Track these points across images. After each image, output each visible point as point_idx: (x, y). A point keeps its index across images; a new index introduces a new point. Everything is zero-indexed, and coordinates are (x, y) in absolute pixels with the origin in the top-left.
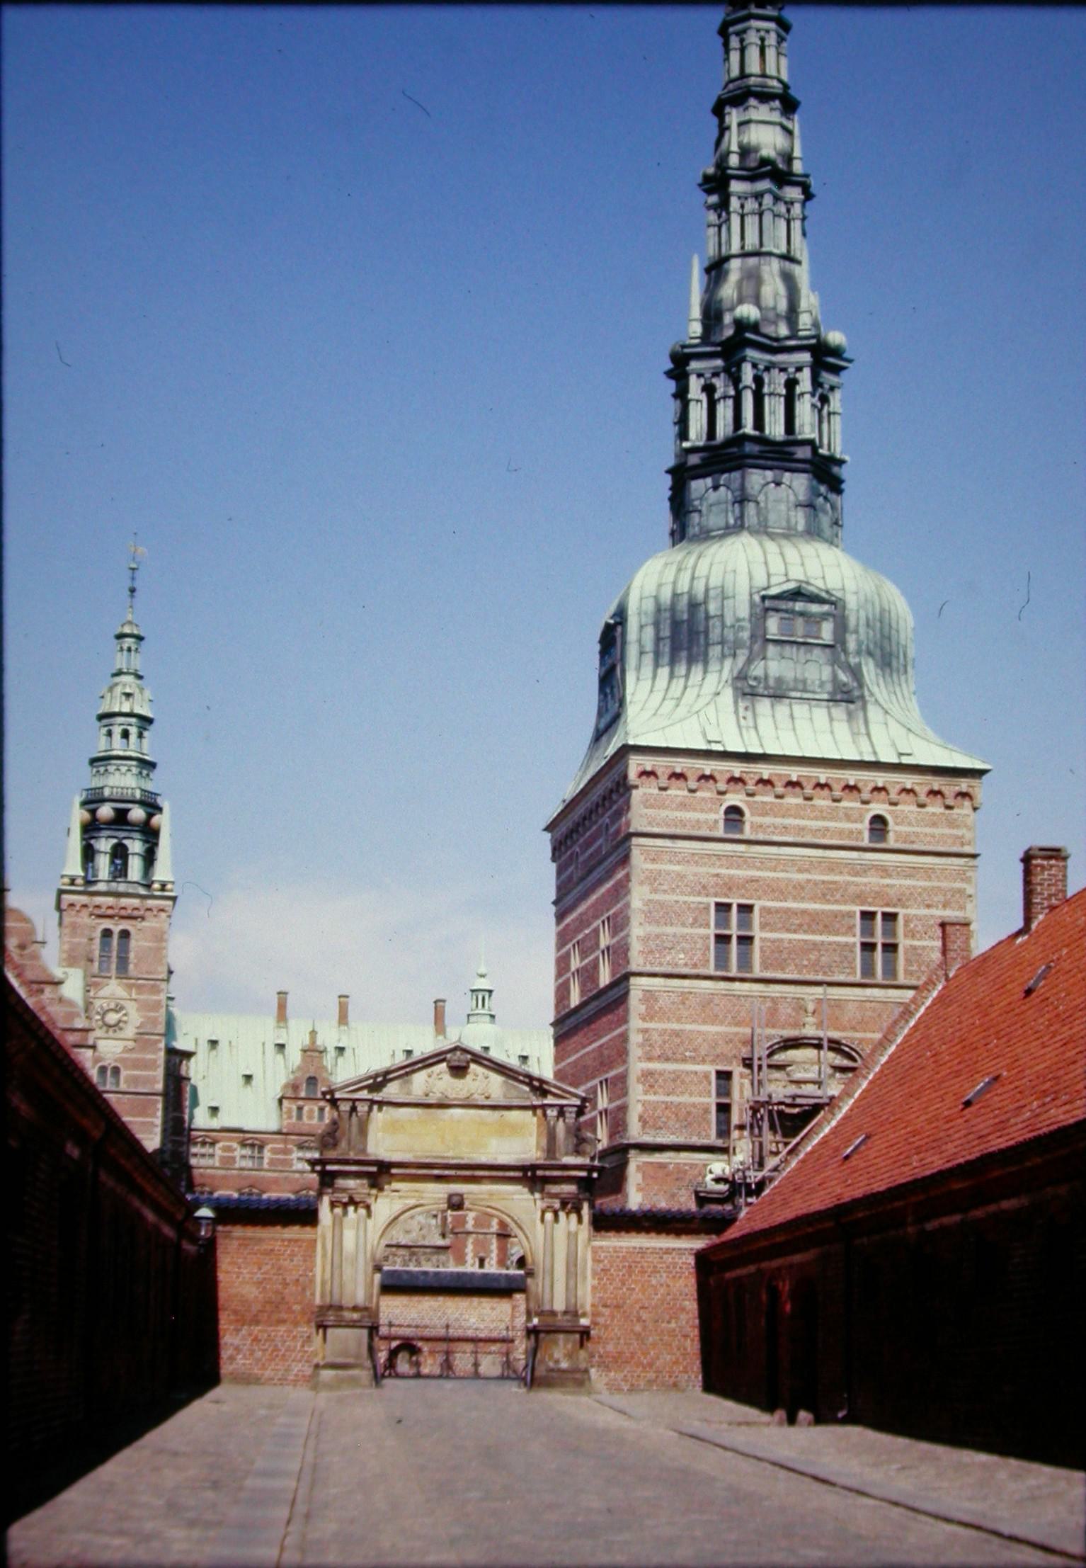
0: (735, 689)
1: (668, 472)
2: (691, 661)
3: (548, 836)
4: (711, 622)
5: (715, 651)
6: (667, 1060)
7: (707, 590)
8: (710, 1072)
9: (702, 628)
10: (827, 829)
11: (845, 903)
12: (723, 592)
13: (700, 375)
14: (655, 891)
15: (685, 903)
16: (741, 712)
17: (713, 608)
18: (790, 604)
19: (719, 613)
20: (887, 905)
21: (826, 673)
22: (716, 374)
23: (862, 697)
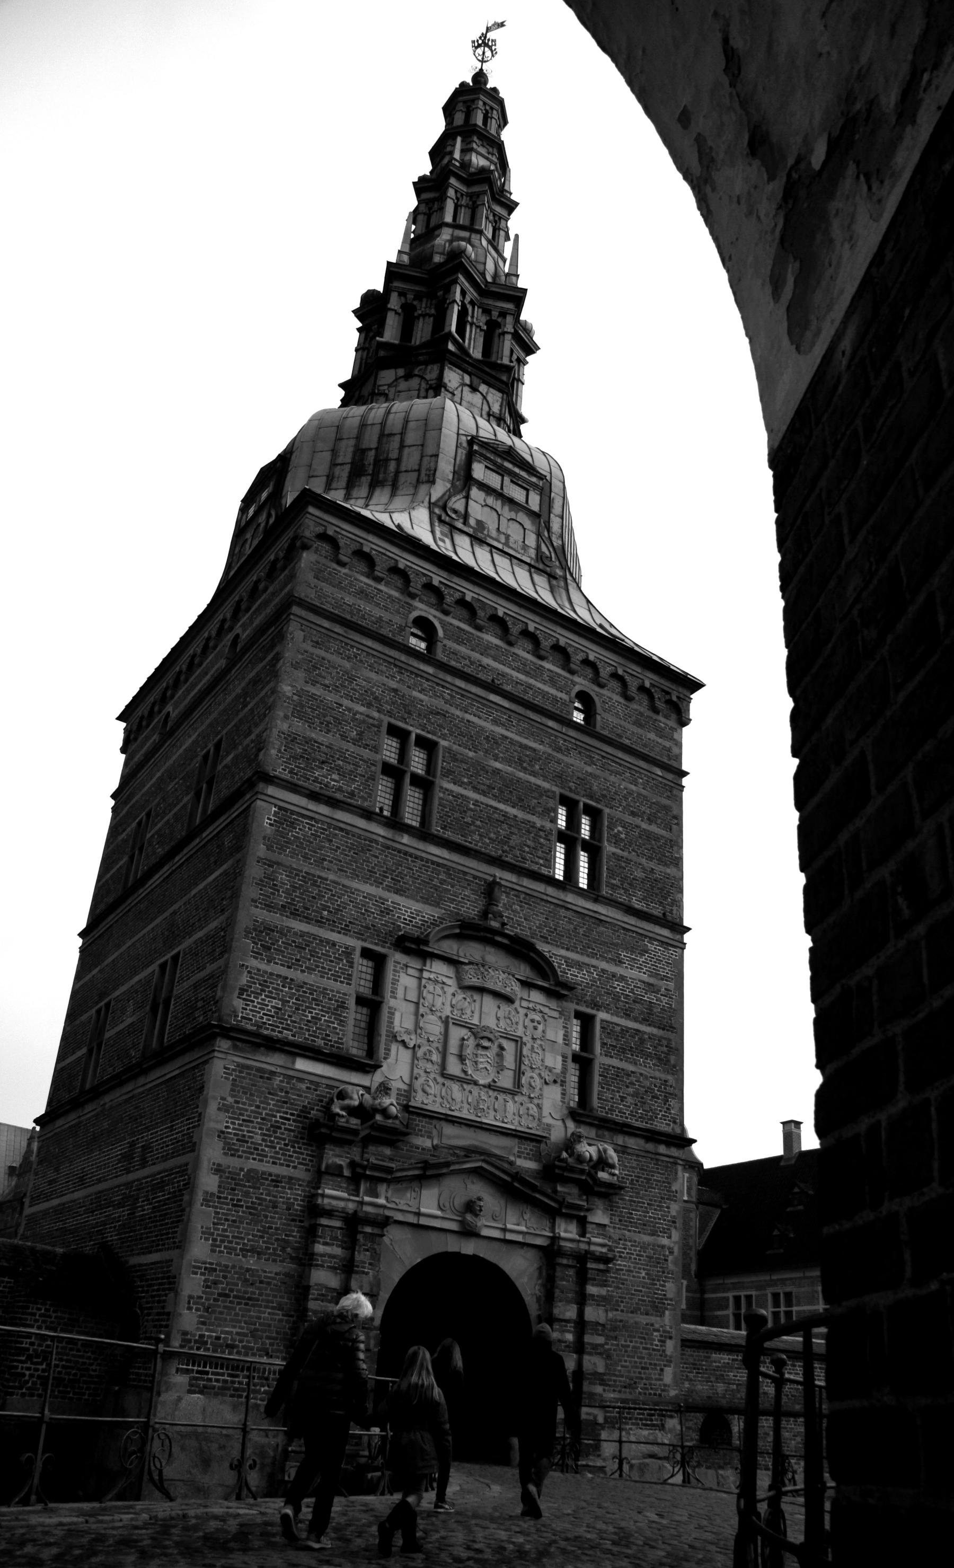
0: (431, 513)
1: (342, 386)
2: (373, 487)
3: (124, 725)
4: (406, 451)
5: (407, 479)
6: (295, 914)
7: (406, 421)
8: (354, 949)
9: (394, 455)
10: (530, 687)
11: (545, 778)
12: (426, 424)
13: (402, 294)
14: (314, 683)
15: (349, 710)
16: (438, 534)
17: (412, 437)
18: (499, 460)
19: (419, 443)
20: (591, 798)
21: (531, 540)
22: (418, 297)
23: (566, 579)
